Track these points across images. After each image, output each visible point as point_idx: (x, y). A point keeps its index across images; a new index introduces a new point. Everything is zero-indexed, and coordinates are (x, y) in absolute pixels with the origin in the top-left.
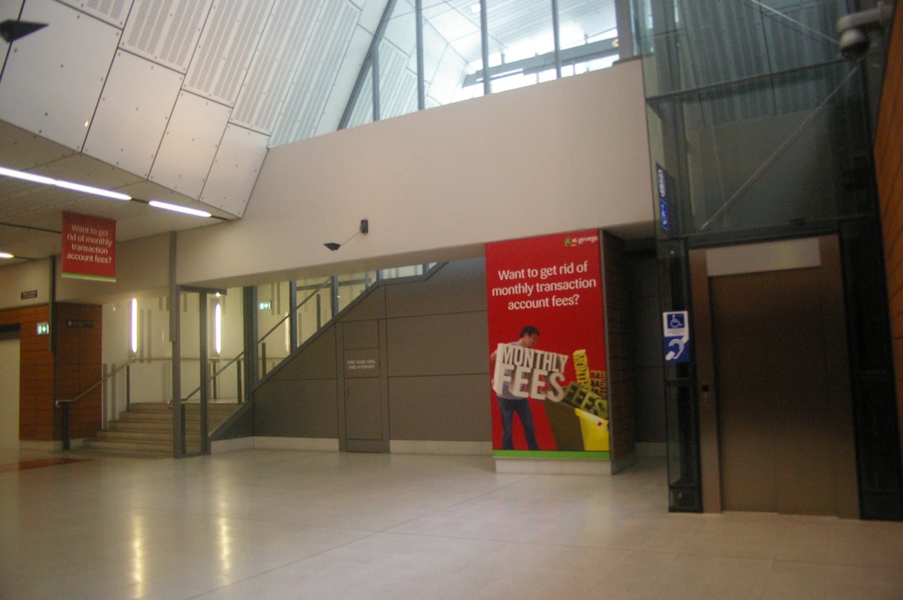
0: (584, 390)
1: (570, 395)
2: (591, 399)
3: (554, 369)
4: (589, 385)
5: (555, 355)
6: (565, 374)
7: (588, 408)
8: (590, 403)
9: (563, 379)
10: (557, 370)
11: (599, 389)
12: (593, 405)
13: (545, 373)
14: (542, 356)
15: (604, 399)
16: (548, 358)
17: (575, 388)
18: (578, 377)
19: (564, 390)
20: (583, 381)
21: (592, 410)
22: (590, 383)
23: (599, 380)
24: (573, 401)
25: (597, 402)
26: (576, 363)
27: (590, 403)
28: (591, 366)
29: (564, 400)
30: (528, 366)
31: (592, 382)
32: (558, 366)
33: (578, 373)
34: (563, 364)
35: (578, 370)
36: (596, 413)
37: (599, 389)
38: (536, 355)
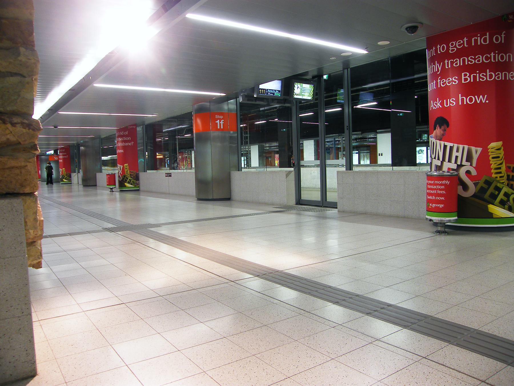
0: (499, 185)
1: (483, 190)
2: (506, 195)
3: (464, 163)
4: (505, 180)
5: (466, 147)
8: (505, 199)
9: (474, 173)
10: (469, 164)
12: (508, 200)
13: (455, 166)
14: (451, 148)
16: (457, 151)
17: (488, 183)
18: (493, 171)
19: (476, 184)
20: (498, 175)
21: (506, 206)
24: (487, 196)
27: (505, 199)
29: (474, 196)
30: (438, 159)
31: (508, 176)
32: (469, 159)
34: (475, 157)
38: (445, 147)
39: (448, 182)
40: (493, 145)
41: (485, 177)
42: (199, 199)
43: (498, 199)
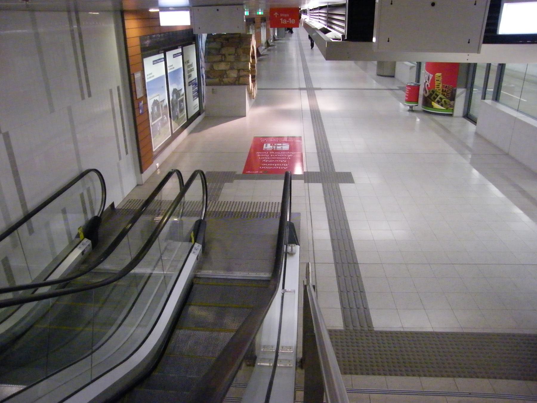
0: (438, 93)
1: (431, 95)
2: (441, 99)
4: (440, 91)
7: (438, 102)
8: (440, 100)
9: (429, 86)
11: (446, 93)
15: (447, 98)
17: (433, 92)
23: (447, 89)
24: (432, 98)
25: (443, 101)
26: (436, 79)
27: (440, 100)
28: (444, 81)
29: (428, 96)
31: (443, 90)
34: (430, 78)
35: (437, 83)
36: (442, 105)
37: (446, 93)
40: (438, 74)
42: (379, 75)
43: (437, 100)
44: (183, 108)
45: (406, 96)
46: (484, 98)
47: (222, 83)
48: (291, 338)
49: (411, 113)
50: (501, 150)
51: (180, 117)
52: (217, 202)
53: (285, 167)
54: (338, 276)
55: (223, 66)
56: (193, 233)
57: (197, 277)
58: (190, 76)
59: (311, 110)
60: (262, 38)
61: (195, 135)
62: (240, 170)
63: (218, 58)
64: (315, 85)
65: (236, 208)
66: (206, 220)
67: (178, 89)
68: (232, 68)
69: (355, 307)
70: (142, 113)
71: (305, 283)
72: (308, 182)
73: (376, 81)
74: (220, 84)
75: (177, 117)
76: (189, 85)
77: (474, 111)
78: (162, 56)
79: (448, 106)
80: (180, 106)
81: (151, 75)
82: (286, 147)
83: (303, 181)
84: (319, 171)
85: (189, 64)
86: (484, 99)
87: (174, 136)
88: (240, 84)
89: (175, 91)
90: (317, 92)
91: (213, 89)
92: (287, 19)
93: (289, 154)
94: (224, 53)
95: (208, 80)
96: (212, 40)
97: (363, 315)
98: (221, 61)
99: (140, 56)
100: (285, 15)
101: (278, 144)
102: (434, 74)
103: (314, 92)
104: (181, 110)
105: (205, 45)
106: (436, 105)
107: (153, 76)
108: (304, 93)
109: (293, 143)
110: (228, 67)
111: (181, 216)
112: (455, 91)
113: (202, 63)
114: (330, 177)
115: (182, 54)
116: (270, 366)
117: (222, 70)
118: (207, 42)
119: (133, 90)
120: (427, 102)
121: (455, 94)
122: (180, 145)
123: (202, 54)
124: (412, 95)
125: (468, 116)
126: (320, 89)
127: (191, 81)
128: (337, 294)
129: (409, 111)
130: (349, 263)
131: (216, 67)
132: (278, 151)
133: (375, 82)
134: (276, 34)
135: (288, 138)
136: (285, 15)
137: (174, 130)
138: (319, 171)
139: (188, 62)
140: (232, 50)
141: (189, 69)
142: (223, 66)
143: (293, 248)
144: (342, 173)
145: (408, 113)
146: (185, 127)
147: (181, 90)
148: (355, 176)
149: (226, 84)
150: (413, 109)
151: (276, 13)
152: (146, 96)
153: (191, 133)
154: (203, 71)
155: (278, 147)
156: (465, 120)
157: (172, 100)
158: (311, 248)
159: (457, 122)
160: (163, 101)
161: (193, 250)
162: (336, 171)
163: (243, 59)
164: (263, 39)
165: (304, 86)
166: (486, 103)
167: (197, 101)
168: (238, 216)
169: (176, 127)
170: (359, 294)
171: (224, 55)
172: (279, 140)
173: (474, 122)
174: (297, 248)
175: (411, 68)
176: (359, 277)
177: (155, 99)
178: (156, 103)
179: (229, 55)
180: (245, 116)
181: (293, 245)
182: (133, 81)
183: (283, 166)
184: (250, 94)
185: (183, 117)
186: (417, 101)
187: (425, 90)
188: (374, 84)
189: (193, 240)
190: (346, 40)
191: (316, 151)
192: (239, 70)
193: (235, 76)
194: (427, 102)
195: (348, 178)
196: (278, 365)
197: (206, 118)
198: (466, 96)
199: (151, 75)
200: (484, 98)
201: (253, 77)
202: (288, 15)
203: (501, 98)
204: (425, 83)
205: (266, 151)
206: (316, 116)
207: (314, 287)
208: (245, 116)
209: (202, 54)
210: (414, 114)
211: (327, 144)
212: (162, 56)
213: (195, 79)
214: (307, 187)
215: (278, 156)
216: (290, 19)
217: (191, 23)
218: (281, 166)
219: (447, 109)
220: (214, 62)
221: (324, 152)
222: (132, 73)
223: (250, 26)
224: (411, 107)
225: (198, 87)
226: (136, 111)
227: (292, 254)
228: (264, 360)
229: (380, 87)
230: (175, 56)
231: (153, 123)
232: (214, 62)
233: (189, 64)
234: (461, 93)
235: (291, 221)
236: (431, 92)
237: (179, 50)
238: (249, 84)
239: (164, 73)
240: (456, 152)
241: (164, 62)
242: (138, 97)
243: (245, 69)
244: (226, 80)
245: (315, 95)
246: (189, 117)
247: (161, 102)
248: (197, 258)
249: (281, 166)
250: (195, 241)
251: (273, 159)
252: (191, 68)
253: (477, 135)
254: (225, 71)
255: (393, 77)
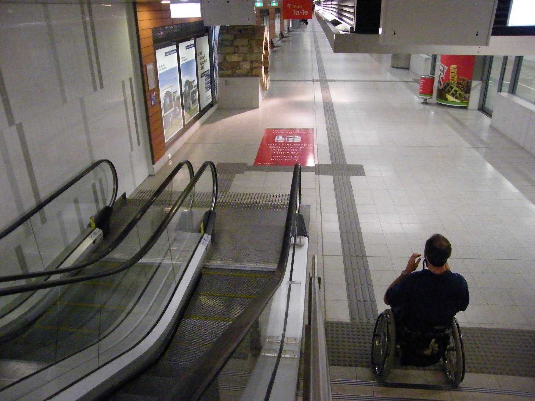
1: (445, 87)
2: (456, 91)
6: (445, 76)
7: (453, 95)
8: (454, 93)
9: (444, 78)
15: (462, 91)
17: (448, 84)
18: (451, 79)
22: (456, 83)
23: (462, 82)
24: (447, 90)
25: (458, 93)
27: (454, 93)
28: (459, 74)
29: (444, 89)
31: (458, 82)
33: (451, 77)
34: (445, 71)
35: (451, 75)
36: (456, 98)
39: (424, 81)
41: (447, 81)
44: (196, 100)
45: (420, 89)
46: (500, 90)
47: (235, 74)
48: (296, 330)
49: (425, 106)
50: (515, 144)
51: (192, 109)
52: (228, 193)
53: (296, 159)
54: (346, 270)
55: (235, 58)
56: (202, 224)
57: (206, 268)
58: (202, 68)
59: (324, 102)
60: (276, 29)
61: (207, 126)
62: (251, 161)
63: (231, 49)
64: (329, 77)
65: (246, 199)
66: (216, 210)
67: (191, 81)
68: (244, 60)
69: (362, 300)
70: (154, 105)
71: (311, 276)
72: (319, 174)
73: (391, 73)
74: (232, 75)
75: (190, 108)
76: (202, 77)
77: (489, 104)
78: (175, 47)
79: (463, 99)
80: (193, 97)
81: (164, 67)
82: (298, 139)
83: (314, 173)
84: (330, 163)
85: (202, 56)
86: (500, 91)
87: (187, 127)
88: (252, 76)
89: (187, 82)
90: (329, 83)
91: (226, 81)
92: (300, 10)
93: (301, 146)
94: (237, 44)
95: (222, 72)
96: (225, 31)
97: (370, 307)
98: (235, 53)
99: (152, 47)
100: (298, 7)
101: (290, 136)
102: (449, 66)
103: (327, 85)
104: (194, 102)
105: (219, 37)
106: (450, 97)
107: (165, 68)
108: (318, 85)
109: (306, 136)
110: (241, 59)
111: (192, 207)
112: (471, 83)
113: (215, 55)
114: (341, 170)
115: (195, 45)
116: (274, 356)
117: (235, 62)
118: (220, 34)
119: (146, 81)
120: (442, 95)
121: (471, 86)
122: (193, 136)
123: (215, 46)
124: (427, 87)
125: (483, 109)
126: (333, 81)
127: (203, 73)
128: (345, 287)
129: (423, 103)
130: (357, 256)
131: (229, 59)
132: (290, 143)
133: (389, 74)
134: (291, 25)
135: (300, 129)
136: (298, 7)
137: (187, 121)
138: (330, 163)
139: (201, 53)
140: (245, 42)
141: (202, 61)
142: (235, 58)
143: (302, 240)
144: (353, 165)
145: (422, 105)
146: (197, 118)
147: (193, 81)
148: (365, 168)
149: (239, 76)
150: (428, 101)
151: (289, 5)
152: (158, 87)
153: (203, 124)
154: (216, 63)
155: (290, 139)
156: (480, 113)
157: (185, 91)
158: (320, 241)
159: (472, 116)
160: (176, 92)
161: (202, 241)
162: (347, 163)
163: (256, 51)
164: (278, 30)
165: (317, 77)
166: (500, 96)
167: (210, 92)
168: (226, 206)
169: (189, 118)
170: (366, 286)
171: (237, 47)
172: (292, 132)
173: (489, 115)
174: (305, 240)
175: (426, 59)
176: (367, 270)
177: (168, 90)
178: (168, 94)
179: (242, 46)
180: (258, 108)
181: (302, 237)
182: (145, 73)
183: (295, 158)
184: (263, 85)
185: (196, 107)
186: (431, 93)
187: (439, 82)
188: (389, 76)
189: (202, 231)
190: (354, 32)
191: (327, 143)
192: (252, 62)
193: (248, 67)
194: (442, 95)
195: (359, 170)
196: (283, 356)
197: (218, 109)
198: (481, 90)
199: (164, 67)
200: (500, 90)
201: (266, 69)
202: (301, 7)
203: (518, 90)
204: (440, 76)
205: (277, 143)
206: (329, 108)
207: (319, 279)
208: (258, 108)
209: (215, 46)
210: (427, 107)
211: (339, 137)
212: (175, 47)
213: (208, 70)
214: (317, 179)
215: (289, 148)
216: (303, 11)
217: (202, 14)
218: (292, 158)
219: (462, 101)
220: (227, 54)
221: (335, 145)
222: (144, 64)
223: (264, 18)
224: (425, 100)
225: (211, 78)
226: (149, 102)
227: (300, 246)
228: (270, 350)
229: (394, 79)
230: (188, 47)
231: (165, 115)
232: (227, 54)
233: (202, 56)
234: (476, 85)
235: (301, 213)
236: (445, 84)
237: (192, 42)
238: (262, 76)
239: (177, 65)
240: (469, 146)
241: (176, 54)
242: (150, 89)
243: (259, 61)
244: (237, 71)
245: (328, 88)
246: (202, 109)
247: (173, 93)
248: (206, 249)
249: (292, 158)
250: (205, 232)
251: (284, 151)
252: (204, 60)
253: (492, 128)
254: (238, 62)
255: (408, 69)
